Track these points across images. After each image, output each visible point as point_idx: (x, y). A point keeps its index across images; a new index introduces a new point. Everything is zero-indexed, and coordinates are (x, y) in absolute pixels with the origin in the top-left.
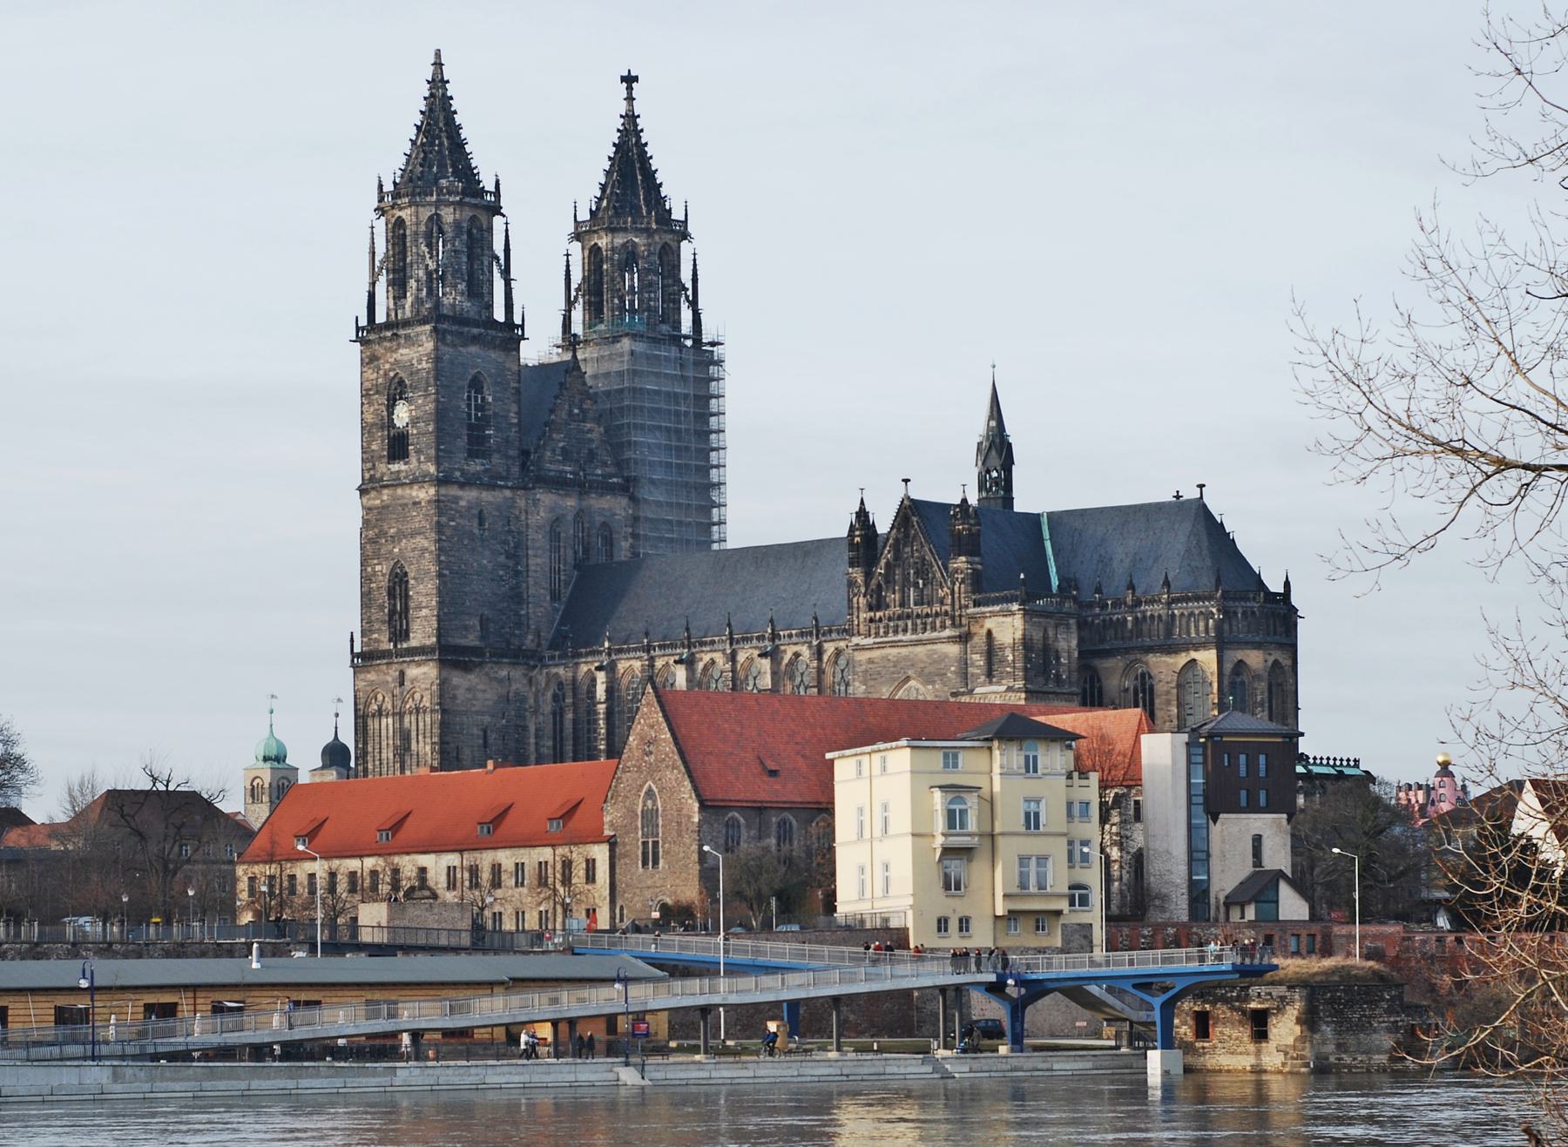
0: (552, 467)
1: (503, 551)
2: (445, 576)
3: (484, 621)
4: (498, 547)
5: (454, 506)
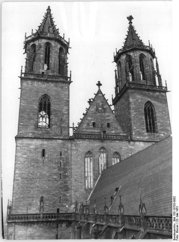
0: (88, 130)
1: (56, 167)
2: (18, 180)
3: (42, 200)
4: (54, 165)
5: (26, 148)
